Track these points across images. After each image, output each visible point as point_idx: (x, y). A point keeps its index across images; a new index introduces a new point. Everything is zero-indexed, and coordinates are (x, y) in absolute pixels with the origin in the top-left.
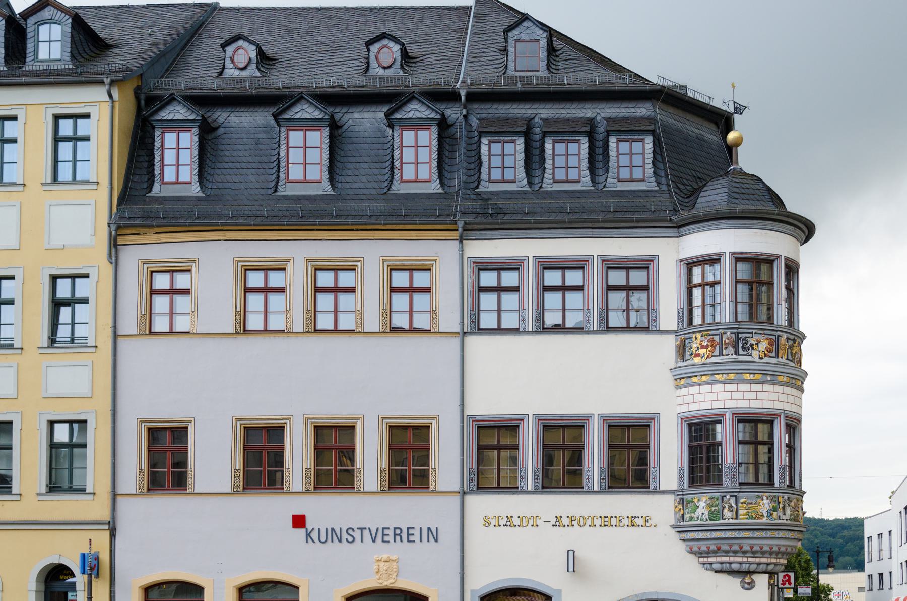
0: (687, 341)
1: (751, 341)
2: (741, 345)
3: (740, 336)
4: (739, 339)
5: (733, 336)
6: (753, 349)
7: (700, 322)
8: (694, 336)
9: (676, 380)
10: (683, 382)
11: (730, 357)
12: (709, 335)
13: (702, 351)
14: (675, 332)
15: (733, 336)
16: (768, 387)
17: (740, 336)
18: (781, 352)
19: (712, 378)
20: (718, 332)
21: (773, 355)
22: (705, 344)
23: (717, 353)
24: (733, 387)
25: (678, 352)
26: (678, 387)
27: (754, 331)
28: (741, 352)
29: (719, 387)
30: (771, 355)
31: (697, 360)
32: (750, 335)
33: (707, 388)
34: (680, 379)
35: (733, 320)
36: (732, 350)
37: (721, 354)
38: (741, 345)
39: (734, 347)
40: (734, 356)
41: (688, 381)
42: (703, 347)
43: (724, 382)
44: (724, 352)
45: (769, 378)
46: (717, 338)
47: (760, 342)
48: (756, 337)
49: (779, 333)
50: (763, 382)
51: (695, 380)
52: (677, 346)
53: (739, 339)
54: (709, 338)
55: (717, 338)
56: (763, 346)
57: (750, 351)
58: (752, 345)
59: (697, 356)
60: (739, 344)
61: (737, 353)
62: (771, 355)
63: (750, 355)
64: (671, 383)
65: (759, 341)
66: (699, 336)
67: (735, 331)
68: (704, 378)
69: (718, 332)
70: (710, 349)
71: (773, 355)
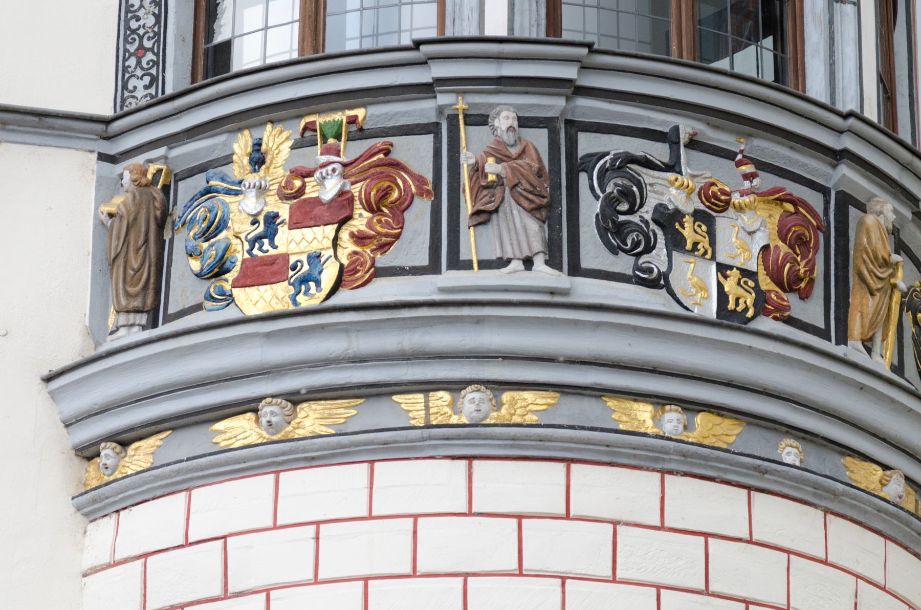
0: (186, 189)
1: (668, 191)
2: (590, 208)
3: (587, 144)
4: (579, 166)
5: (539, 138)
6: (676, 243)
7: (285, 44)
8: (241, 145)
9: (88, 453)
10: (141, 455)
11: (513, 275)
12: (362, 133)
13: (293, 242)
14: (101, 127)
15: (539, 138)
16: (780, 519)
17: (587, 144)
18: (863, 308)
19: (378, 414)
20: (422, 110)
21: (812, 311)
22: (330, 188)
23: (413, 246)
24: (537, 484)
25: (111, 261)
26: (96, 505)
27: (687, 126)
28: (593, 252)
29: (430, 482)
30: (797, 308)
31: (255, 300)
32: (659, 152)
33: (316, 490)
34: (124, 440)
35: (532, 24)
36: (522, 229)
37: (445, 253)
38: (590, 208)
39: (544, 211)
40: (544, 275)
41: (188, 443)
42: (307, 214)
43: (468, 445)
44: (472, 244)
45: (790, 452)
46: (416, 153)
47: (723, 205)
48: (697, 169)
49: (846, 176)
50: (753, 477)
51: (240, 430)
52: (107, 224)
53: (577, 165)
54: (353, 150)
55: (416, 153)
56: (747, 234)
57: (658, 259)
58: (668, 219)
59: (263, 271)
60: (587, 198)
61: (562, 252)
62: (797, 308)
63: (658, 281)
64: (52, 475)
65: (714, 205)
66: (278, 141)
67: (552, 105)
68: (312, 419)
69: (422, 110)
70: (361, 221)
71: (812, 311)
